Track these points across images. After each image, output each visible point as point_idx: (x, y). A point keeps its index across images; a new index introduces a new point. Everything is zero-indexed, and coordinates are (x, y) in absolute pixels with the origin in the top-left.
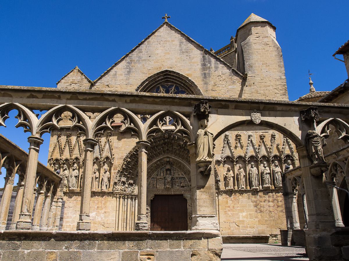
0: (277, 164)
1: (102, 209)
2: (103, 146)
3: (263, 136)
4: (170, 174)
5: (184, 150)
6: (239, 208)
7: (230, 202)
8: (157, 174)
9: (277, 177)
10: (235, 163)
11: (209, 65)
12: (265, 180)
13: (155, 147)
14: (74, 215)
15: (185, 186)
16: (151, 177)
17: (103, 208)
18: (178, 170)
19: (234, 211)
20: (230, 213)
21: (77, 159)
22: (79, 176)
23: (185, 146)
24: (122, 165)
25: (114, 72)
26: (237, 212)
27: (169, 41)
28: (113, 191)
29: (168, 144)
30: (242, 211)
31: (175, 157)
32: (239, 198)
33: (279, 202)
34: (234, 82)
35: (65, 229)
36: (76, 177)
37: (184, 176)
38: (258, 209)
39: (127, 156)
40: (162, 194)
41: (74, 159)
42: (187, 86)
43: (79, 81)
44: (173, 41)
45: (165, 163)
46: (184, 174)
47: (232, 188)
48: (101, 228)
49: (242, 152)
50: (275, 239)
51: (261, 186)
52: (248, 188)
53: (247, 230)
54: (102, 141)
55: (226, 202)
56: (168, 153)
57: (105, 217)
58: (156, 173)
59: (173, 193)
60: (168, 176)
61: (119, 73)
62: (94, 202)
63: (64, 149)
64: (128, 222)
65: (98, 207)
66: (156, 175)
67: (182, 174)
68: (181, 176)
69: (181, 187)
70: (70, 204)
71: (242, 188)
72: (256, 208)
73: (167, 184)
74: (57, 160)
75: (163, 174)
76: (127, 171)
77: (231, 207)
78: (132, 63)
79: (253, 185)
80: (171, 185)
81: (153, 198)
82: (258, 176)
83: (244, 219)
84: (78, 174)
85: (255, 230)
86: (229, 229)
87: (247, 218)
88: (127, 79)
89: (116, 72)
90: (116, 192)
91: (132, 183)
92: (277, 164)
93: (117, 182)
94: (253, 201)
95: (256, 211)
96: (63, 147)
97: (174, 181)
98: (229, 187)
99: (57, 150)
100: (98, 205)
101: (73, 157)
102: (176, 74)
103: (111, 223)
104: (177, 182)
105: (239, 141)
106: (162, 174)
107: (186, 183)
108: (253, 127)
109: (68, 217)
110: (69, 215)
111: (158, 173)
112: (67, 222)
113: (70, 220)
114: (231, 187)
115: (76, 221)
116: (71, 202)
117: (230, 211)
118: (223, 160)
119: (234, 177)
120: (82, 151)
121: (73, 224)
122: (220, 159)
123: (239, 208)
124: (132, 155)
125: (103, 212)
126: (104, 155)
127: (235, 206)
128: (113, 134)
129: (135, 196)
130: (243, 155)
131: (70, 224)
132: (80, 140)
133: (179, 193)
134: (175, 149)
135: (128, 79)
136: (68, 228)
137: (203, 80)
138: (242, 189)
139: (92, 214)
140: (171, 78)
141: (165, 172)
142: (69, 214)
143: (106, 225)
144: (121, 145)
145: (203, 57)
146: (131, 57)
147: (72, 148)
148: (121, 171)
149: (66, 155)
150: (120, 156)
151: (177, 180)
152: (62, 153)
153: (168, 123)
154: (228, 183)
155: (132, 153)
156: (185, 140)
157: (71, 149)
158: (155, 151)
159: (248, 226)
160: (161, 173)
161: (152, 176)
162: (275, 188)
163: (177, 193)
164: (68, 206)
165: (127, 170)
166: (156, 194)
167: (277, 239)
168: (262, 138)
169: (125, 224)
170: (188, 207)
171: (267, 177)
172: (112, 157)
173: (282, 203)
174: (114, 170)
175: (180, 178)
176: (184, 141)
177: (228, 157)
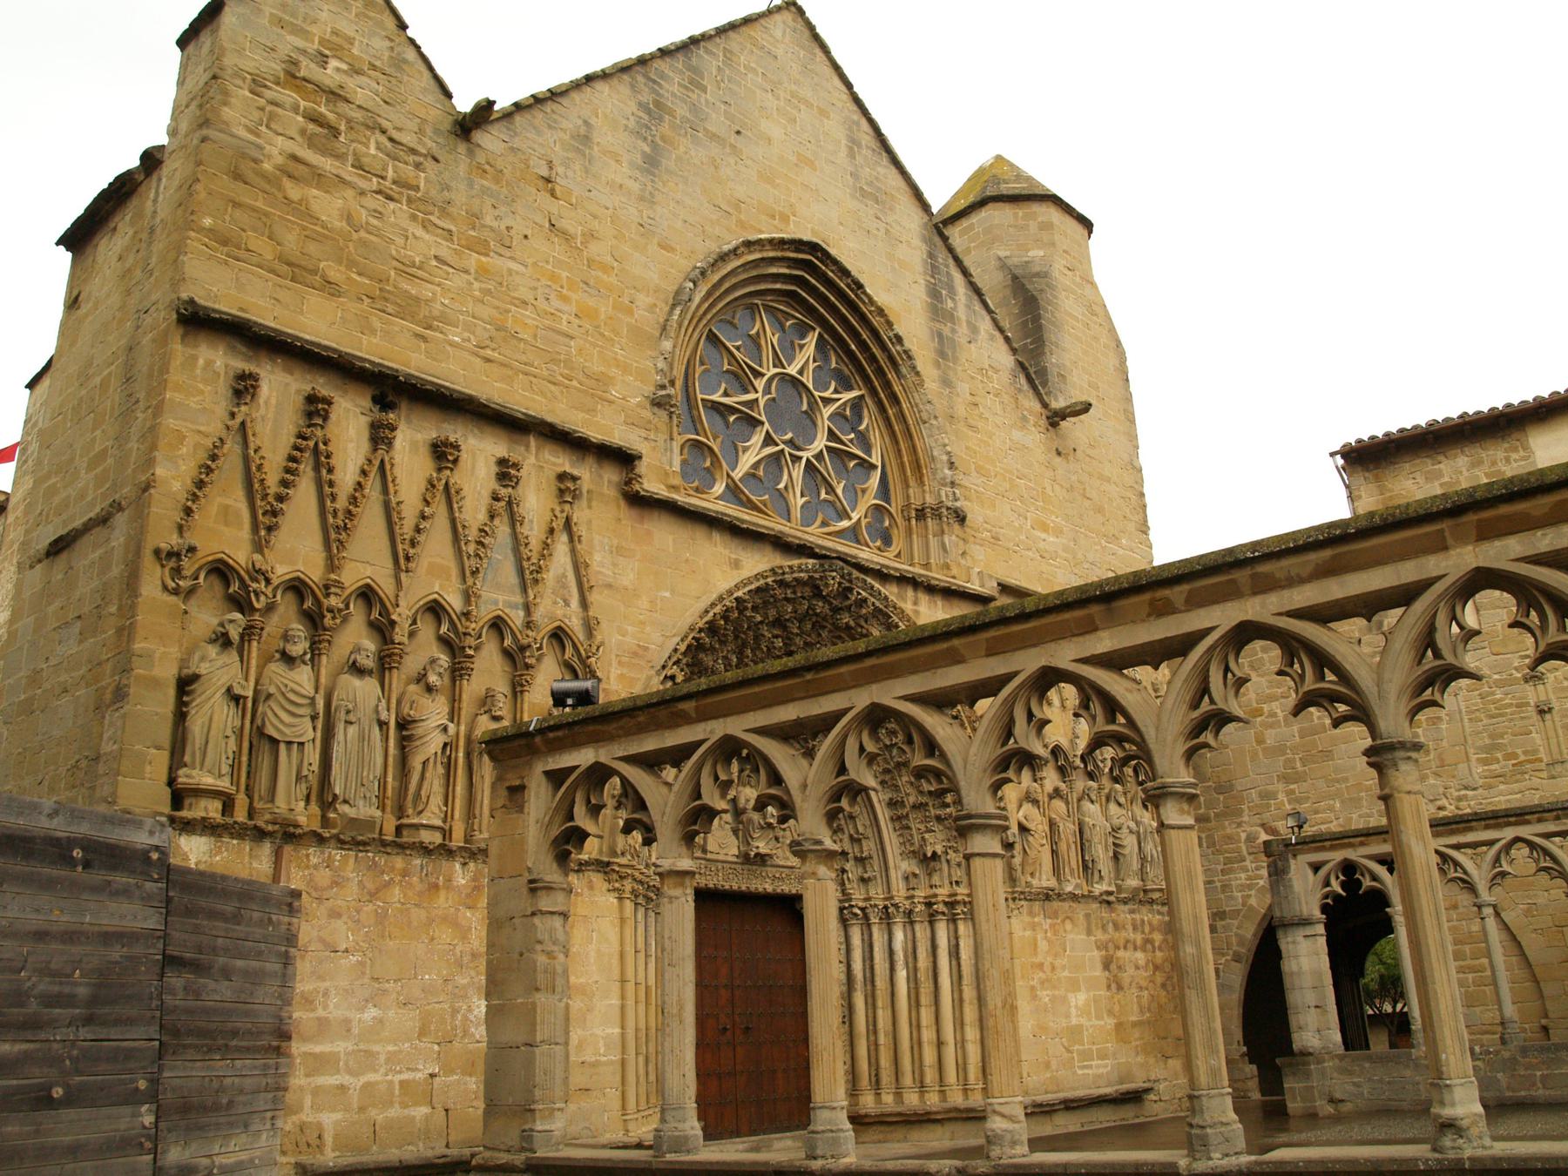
6: (1066, 973)
7: (1043, 945)
11: (950, 304)
14: (372, 1013)
19: (1054, 987)
25: (580, 122)
27: (809, 105)
30: (1074, 986)
34: (1024, 419)
35: (307, 1116)
42: (873, 359)
43: (378, 63)
44: (823, 113)
47: (1053, 883)
53: (1090, 1067)
59: (770, 889)
61: (605, 137)
70: (339, 924)
74: (221, 570)
77: (1047, 968)
78: (661, 119)
86: (1047, 1065)
88: (641, 199)
89: (586, 122)
95: (1109, 987)
96: (272, 479)
99: (229, 496)
102: (848, 286)
109: (323, 1023)
110: (335, 1009)
112: (322, 1063)
113: (341, 1047)
114: (1045, 880)
115: (382, 1058)
116: (339, 915)
121: (363, 1079)
123: (1066, 973)
127: (1058, 962)
131: (346, 1079)
135: (647, 199)
136: (333, 1110)
137: (938, 365)
140: (812, 290)
142: (334, 1000)
145: (931, 255)
146: (654, 82)
149: (297, 550)
153: (797, 513)
164: (322, 941)
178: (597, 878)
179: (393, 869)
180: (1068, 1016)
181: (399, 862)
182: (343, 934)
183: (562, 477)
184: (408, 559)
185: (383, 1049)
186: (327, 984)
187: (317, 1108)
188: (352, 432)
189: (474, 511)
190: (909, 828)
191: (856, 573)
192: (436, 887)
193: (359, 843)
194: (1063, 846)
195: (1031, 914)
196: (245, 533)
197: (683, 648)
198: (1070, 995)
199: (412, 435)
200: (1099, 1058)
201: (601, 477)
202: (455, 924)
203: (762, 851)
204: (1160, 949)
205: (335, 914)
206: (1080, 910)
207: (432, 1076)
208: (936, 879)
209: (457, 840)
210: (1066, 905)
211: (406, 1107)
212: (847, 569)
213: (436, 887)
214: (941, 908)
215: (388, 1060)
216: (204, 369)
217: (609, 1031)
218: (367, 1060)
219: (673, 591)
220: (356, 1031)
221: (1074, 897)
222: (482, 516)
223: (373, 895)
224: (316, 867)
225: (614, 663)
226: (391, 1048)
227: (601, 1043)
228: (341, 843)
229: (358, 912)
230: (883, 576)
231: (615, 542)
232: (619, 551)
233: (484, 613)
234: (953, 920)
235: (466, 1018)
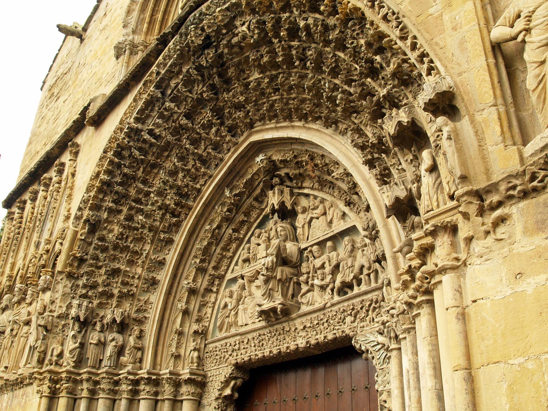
16: (221, 278)
18: (323, 201)
68: (339, 226)
133: (330, 337)
161: (229, 276)
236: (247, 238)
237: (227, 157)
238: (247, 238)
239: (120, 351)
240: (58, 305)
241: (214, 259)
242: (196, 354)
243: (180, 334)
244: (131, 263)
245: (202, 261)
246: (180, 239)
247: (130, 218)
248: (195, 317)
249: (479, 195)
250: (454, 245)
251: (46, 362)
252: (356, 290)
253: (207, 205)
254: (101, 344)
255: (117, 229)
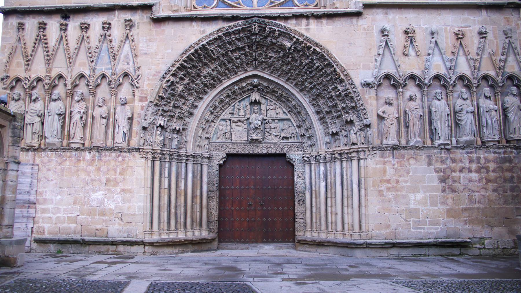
0: (489, 94)
1: (116, 184)
2: (116, 49)
3: (461, 33)
4: (260, 112)
5: (292, 61)
6: (409, 184)
7: (390, 171)
8: (231, 112)
9: (489, 122)
10: (401, 90)
12: (464, 125)
13: (230, 52)
14: (59, 197)
15: (291, 138)
16: (218, 117)
17: (118, 181)
19: (397, 191)
20: (390, 193)
21: (60, 77)
22: (65, 114)
23: (294, 51)
24: (157, 90)
26: (404, 193)
28: (140, 146)
29: (257, 48)
30: (415, 190)
31: (270, 75)
32: (409, 164)
33: (491, 174)
36: (60, 115)
37: (289, 116)
38: (447, 187)
39: (169, 71)
40: (243, 152)
41: (55, 78)
45: (248, 90)
46: (289, 112)
47: (396, 142)
48: (115, 224)
49: (417, 67)
50: (481, 247)
51: (454, 139)
52: (429, 143)
53: (424, 229)
54: (114, 39)
55: (383, 172)
56: (256, 68)
57: (124, 200)
58: (230, 109)
59: (265, 152)
60: (254, 116)
62: (98, 169)
63: (31, 56)
64: (173, 210)
65: (108, 180)
66: (230, 113)
67: (284, 113)
69: (283, 139)
71: (417, 142)
72: (443, 184)
73: (253, 133)
75: (245, 113)
76: (169, 103)
79: (439, 137)
80: (260, 135)
81: (224, 162)
82: (450, 118)
83: (419, 207)
84: (64, 110)
85: (439, 230)
86: (388, 227)
87: (425, 204)
90: (145, 147)
91: (179, 129)
92: (488, 94)
93: (147, 126)
94: (437, 170)
95: (444, 191)
96: (29, 52)
97: (267, 126)
98: (390, 139)
99: (19, 59)
100: (107, 176)
101: (54, 74)
103: (137, 215)
104: (274, 128)
105: (411, 42)
106: (242, 113)
107: (294, 132)
108: (440, 15)
109: (45, 200)
110: (48, 196)
111: (233, 110)
112: (44, 211)
113: (50, 206)
114: (392, 140)
115: (62, 210)
117: (391, 189)
118: (376, 83)
119: (398, 119)
120: (71, 60)
121: (56, 216)
122: (370, 80)
123: (409, 184)
124: (178, 68)
125: (119, 190)
126: (121, 67)
127: (401, 179)
128: (136, 24)
129: (187, 156)
130: (417, 72)
131: (52, 215)
132: (66, 36)
133: (278, 152)
134: (272, 59)
136: (48, 223)
138: (417, 145)
139: (97, 194)
141: (248, 107)
142: (48, 193)
143: (126, 219)
144: (155, 48)
147: (50, 53)
148: (155, 103)
149: (38, 69)
150: (153, 71)
151: (273, 125)
152: (28, 65)
154: (388, 132)
155: (180, 64)
156: (294, 37)
157: (48, 56)
158: (229, 62)
159: (428, 220)
160: (239, 110)
161: (222, 117)
162: (483, 142)
163: (274, 152)
164: (45, 177)
165: (168, 101)
166: (231, 152)
167: (483, 246)
168: (459, 36)
169: (166, 214)
170: (295, 180)
171: (469, 121)
172: (135, 73)
173: (495, 174)
174: (141, 100)
175: (279, 120)
176: (292, 39)
177: (387, 77)
178: (136, 154)
179: (66, 156)
180: (408, 204)
181: (68, 154)
182: (51, 175)
183: (126, 21)
184: (70, 63)
185: (62, 208)
186: (46, 189)
187: (43, 222)
188: (54, 30)
189: (73, 44)
190: (326, 123)
191: (266, 21)
192: (80, 160)
193: (54, 149)
194: (411, 124)
195: (382, 156)
196: (23, 68)
197: (174, 68)
198: (410, 195)
199: (74, 24)
200: (430, 225)
201: (143, 16)
202: (86, 171)
203: (254, 138)
204: (493, 171)
205: (49, 170)
206: (423, 155)
207: (78, 215)
208: (337, 144)
209: (86, 146)
210: (412, 152)
211: (69, 224)
212: (261, 20)
213: (80, 160)
214: (337, 156)
215: (64, 211)
216: (11, 25)
217: (140, 204)
218: (58, 210)
219: (172, 49)
220: (54, 202)
221: (416, 148)
222: (97, 43)
223: (60, 164)
224: (43, 157)
225: (146, 80)
226: (65, 207)
227: (136, 208)
228: (51, 150)
229: (56, 169)
230: (286, 18)
231: (148, 38)
232: (150, 40)
233: (98, 73)
234: (342, 162)
235: (88, 199)
236: (233, 105)
237: (239, 73)
238: (233, 105)
239: (179, 143)
240: (149, 117)
241: (218, 109)
242: (207, 147)
243: (201, 137)
244: (184, 104)
245: (214, 109)
246: (208, 99)
247: (188, 84)
248: (206, 131)
249: (373, 147)
250: (364, 155)
251: (146, 144)
252: (290, 140)
253: (224, 89)
254: (171, 139)
255: (181, 88)
